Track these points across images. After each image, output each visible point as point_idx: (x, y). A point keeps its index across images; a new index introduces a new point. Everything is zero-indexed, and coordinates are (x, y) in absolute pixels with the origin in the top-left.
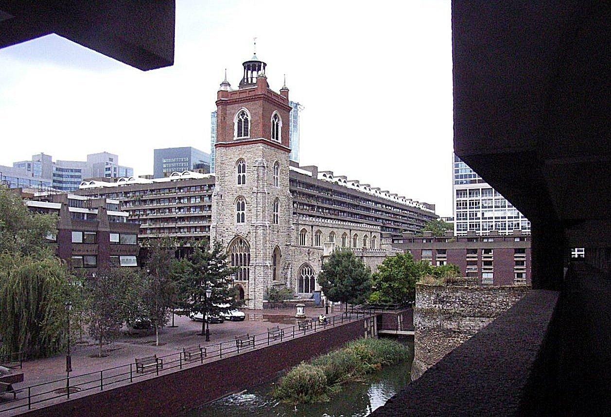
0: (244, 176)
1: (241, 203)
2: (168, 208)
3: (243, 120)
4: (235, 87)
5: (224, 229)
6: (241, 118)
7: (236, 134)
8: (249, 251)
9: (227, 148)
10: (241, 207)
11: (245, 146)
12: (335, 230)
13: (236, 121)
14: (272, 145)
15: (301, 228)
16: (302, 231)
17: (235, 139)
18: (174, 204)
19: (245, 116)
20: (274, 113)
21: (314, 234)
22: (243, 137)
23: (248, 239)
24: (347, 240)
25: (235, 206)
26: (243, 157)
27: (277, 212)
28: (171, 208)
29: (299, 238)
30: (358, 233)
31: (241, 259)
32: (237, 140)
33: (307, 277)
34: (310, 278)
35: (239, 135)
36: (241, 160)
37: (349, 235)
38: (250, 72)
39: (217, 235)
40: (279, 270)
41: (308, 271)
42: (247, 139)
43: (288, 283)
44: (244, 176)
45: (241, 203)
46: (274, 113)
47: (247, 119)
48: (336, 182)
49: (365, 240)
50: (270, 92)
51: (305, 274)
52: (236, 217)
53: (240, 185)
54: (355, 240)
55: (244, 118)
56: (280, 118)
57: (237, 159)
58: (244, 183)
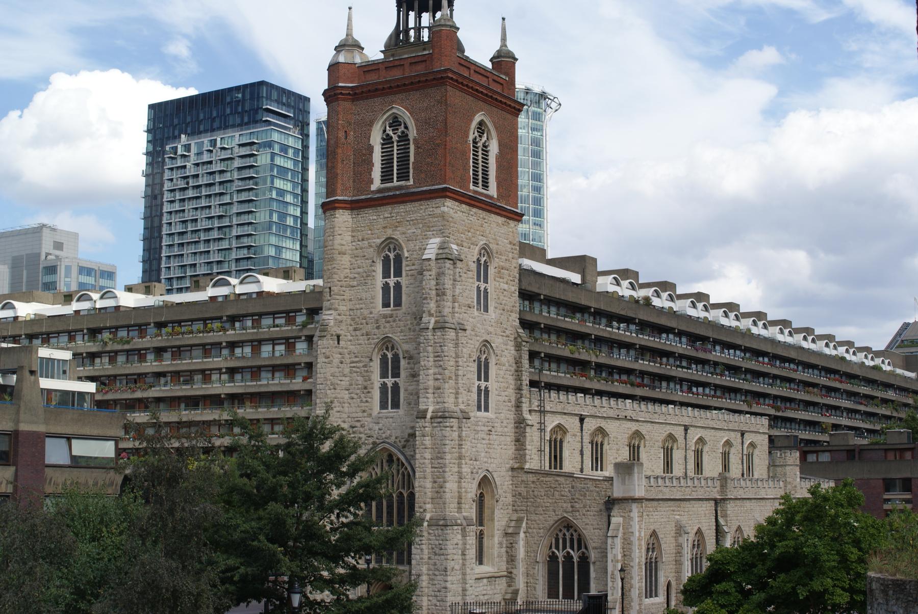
0: (398, 286)
2: (203, 371)
3: (395, 138)
4: (374, 50)
6: (391, 133)
7: (377, 173)
9: (355, 212)
10: (391, 367)
11: (402, 207)
12: (644, 429)
13: (376, 139)
14: (474, 202)
15: (551, 422)
16: (553, 431)
17: (374, 187)
18: (217, 361)
19: (402, 128)
20: (478, 118)
21: (587, 439)
22: (396, 183)
24: (677, 455)
25: (376, 366)
26: (397, 235)
27: (487, 380)
28: (211, 370)
29: (547, 449)
30: (707, 435)
31: (390, 507)
32: (379, 191)
33: (568, 557)
34: (576, 559)
35: (386, 176)
36: (390, 243)
37: (681, 439)
38: (412, 15)
40: (493, 536)
41: (572, 540)
42: (407, 187)
46: (478, 118)
47: (404, 138)
48: (647, 300)
49: (726, 457)
50: (468, 64)
51: (564, 547)
53: (387, 311)
54: (699, 454)
56: (494, 133)
57: (379, 241)
58: (398, 304)
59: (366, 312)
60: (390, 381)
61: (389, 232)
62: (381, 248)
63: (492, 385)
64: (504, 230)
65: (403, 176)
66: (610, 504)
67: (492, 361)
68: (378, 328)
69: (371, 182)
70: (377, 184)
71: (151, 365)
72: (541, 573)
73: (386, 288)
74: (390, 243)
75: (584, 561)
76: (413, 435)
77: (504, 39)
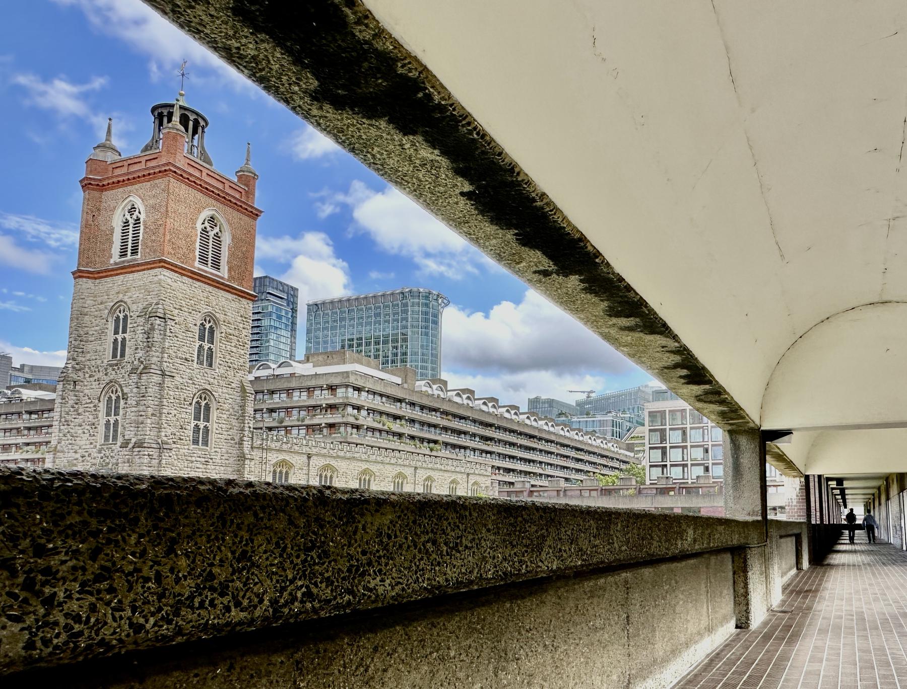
0: (124, 339)
1: (114, 398)
3: (131, 222)
5: (78, 456)
9: (98, 281)
14: (196, 276)
19: (137, 213)
25: (102, 406)
26: (126, 299)
32: (116, 264)
42: (135, 260)
44: (124, 339)
45: (114, 398)
46: (206, 214)
52: (101, 429)
55: (134, 217)
56: (226, 226)
59: (99, 362)
61: (121, 296)
63: (213, 426)
64: (235, 305)
65: (135, 252)
67: (214, 406)
68: (106, 375)
70: (115, 258)
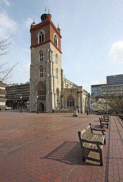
0: (43, 58)
1: (41, 69)
3: (41, 35)
8: (46, 88)
10: (42, 70)
19: (42, 33)
23: (45, 83)
25: (39, 70)
31: (42, 92)
33: (71, 101)
36: (41, 51)
39: (32, 83)
43: (63, 103)
44: (43, 58)
45: (41, 69)
47: (43, 35)
52: (40, 75)
58: (43, 60)
60: (42, 73)
62: (40, 52)
65: (43, 40)
66: (78, 92)
69: (38, 43)
71: (22, 90)
72: (66, 104)
73: (41, 58)
74: (41, 51)
75: (73, 102)
76: (46, 80)
77: (58, 27)
